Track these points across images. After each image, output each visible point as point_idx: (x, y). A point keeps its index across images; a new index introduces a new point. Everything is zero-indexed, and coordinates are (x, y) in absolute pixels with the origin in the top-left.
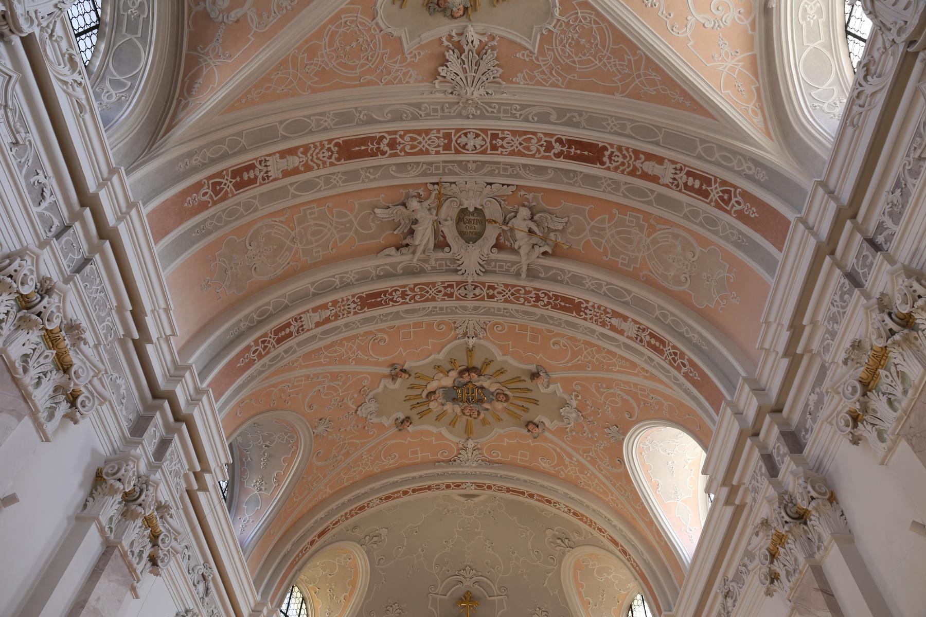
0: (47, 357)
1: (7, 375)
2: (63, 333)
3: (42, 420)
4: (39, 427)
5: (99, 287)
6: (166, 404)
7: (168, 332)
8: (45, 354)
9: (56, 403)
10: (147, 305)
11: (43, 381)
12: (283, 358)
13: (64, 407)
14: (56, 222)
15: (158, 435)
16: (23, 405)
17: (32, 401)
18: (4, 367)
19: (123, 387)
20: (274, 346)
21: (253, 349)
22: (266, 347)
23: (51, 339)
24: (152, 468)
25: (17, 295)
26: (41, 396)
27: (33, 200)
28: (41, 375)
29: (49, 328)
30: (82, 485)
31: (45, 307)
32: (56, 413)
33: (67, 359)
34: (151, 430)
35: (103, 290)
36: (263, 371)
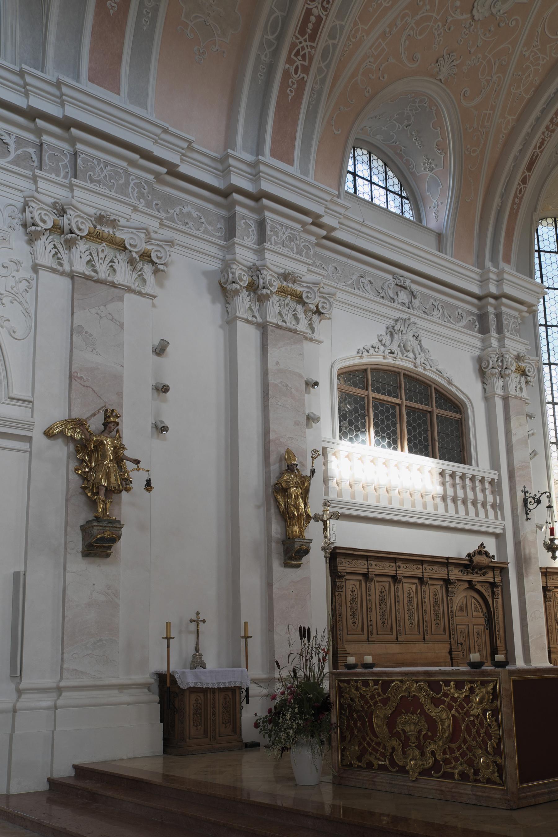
0: (103, 251)
1: (89, 282)
2: (98, 227)
4: (140, 294)
5: (102, 165)
8: (100, 250)
9: (140, 271)
11: (115, 267)
12: (335, 46)
13: (148, 269)
15: (251, 222)
16: (116, 290)
17: (119, 284)
18: (84, 280)
19: (193, 211)
20: (312, 47)
21: (292, 69)
22: (304, 57)
23: (94, 236)
24: (260, 252)
25: (48, 232)
26: (123, 275)
28: (111, 264)
31: (69, 224)
32: (145, 277)
33: (118, 240)
34: (240, 225)
35: (106, 164)
36: (325, 77)
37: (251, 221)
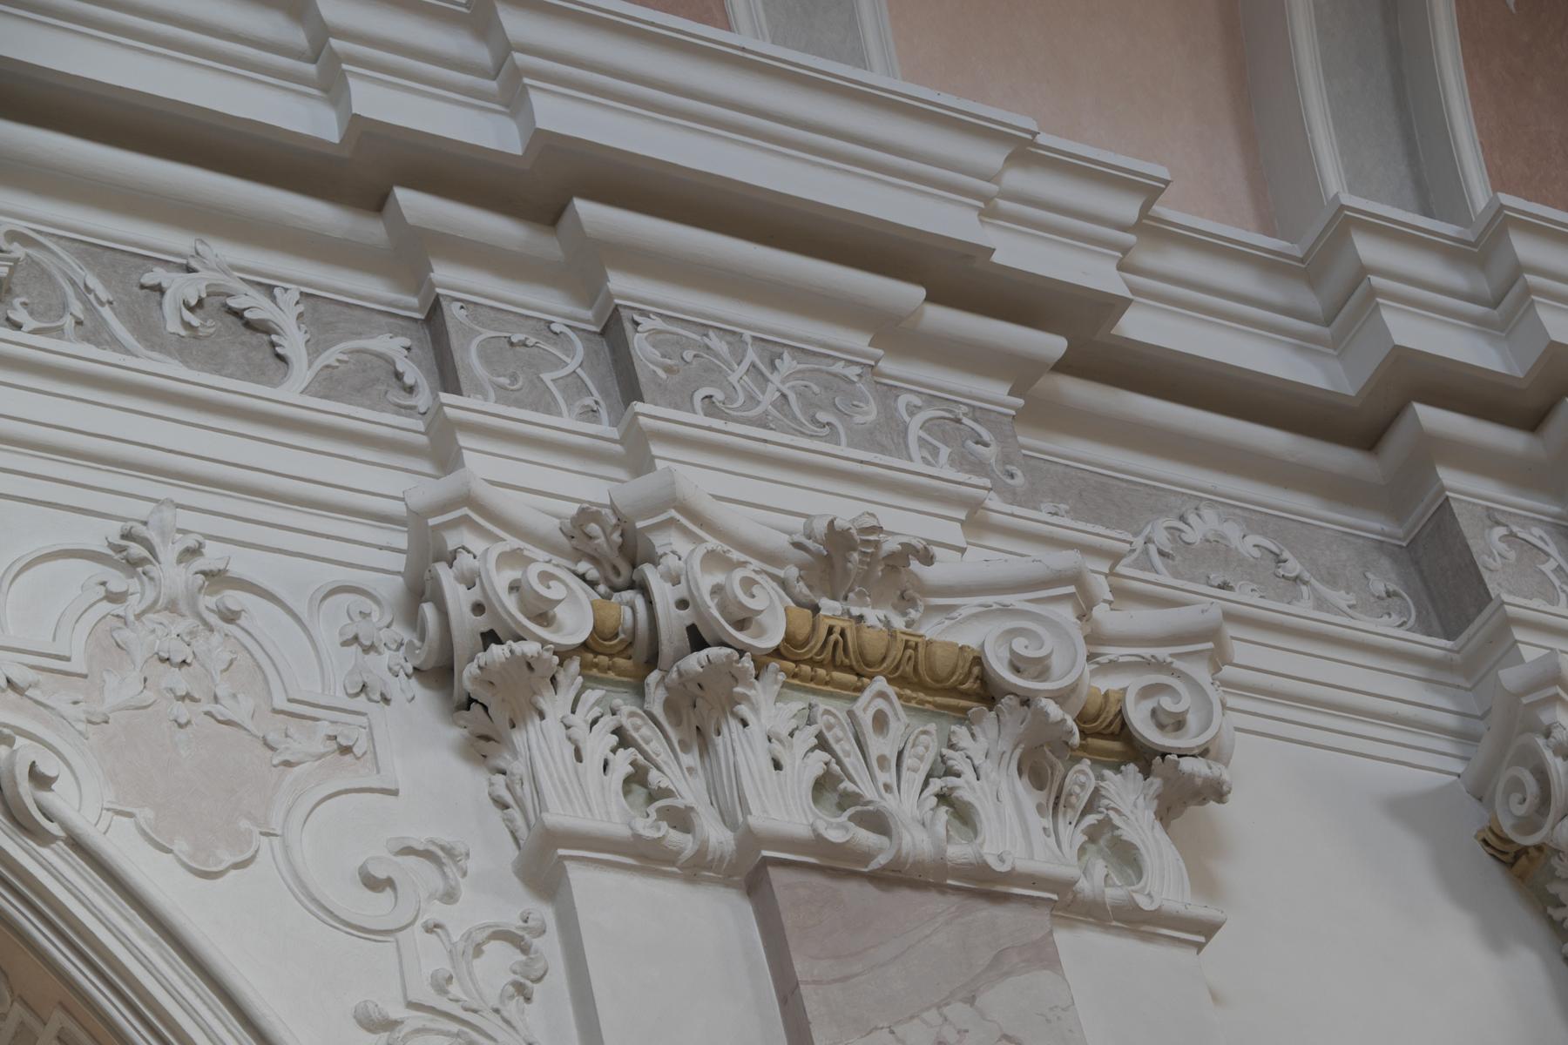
0: (880, 721)
1: (851, 890)
2: (829, 606)
3: (1114, 893)
4: (1134, 921)
5: (751, 355)
6: (1429, 416)
7: (1128, 208)
8: (866, 719)
9: (1089, 808)
10: (951, 221)
11: (965, 794)
13: (1129, 797)
14: (391, 345)
15: (1535, 534)
16: (1003, 915)
17: (1012, 877)
18: (817, 880)
19: (1232, 531)
23: (819, 660)
25: (574, 665)
26: (1014, 830)
27: (255, 373)
28: (936, 785)
29: (773, 639)
30: (1495, 940)
31: (682, 604)
32: (1128, 833)
33: (942, 661)
34: (1491, 550)
35: (772, 350)
37: (1537, 531)
